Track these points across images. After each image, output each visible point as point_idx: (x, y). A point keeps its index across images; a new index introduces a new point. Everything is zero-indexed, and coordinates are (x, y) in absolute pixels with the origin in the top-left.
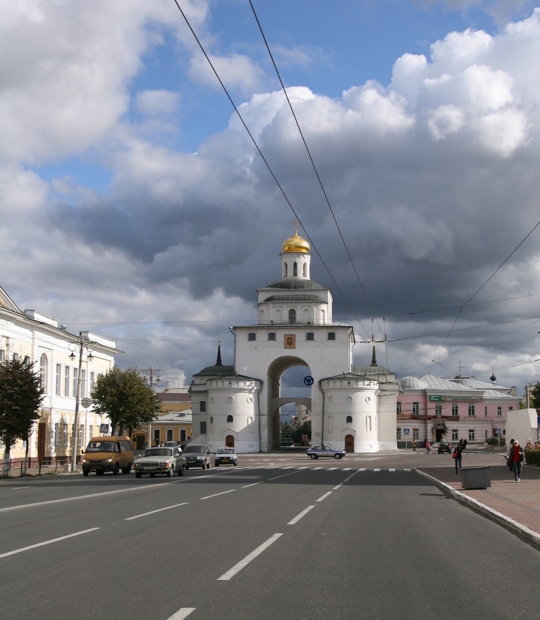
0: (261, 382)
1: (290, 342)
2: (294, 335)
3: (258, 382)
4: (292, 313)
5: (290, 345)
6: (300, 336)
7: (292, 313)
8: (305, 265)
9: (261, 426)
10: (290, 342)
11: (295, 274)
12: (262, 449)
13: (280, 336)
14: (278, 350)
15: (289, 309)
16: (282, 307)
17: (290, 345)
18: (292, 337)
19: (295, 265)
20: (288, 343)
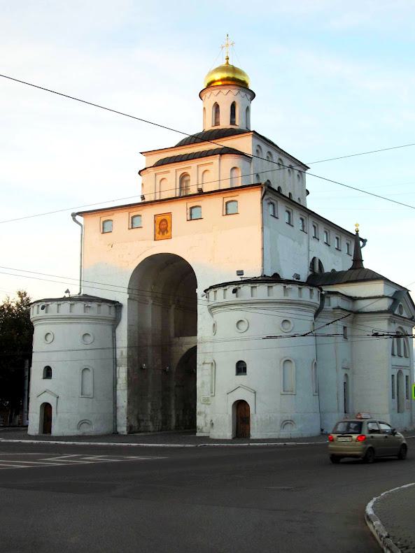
0: (117, 305)
1: (163, 228)
2: (170, 214)
3: (105, 307)
4: (184, 177)
5: (163, 234)
6: (178, 211)
7: (184, 177)
8: (233, 106)
9: (118, 386)
10: (163, 228)
11: (217, 123)
12: (119, 430)
13: (148, 216)
14: (148, 246)
15: (179, 173)
16: (168, 172)
17: (163, 234)
18: (167, 217)
19: (217, 106)
20: (160, 229)
